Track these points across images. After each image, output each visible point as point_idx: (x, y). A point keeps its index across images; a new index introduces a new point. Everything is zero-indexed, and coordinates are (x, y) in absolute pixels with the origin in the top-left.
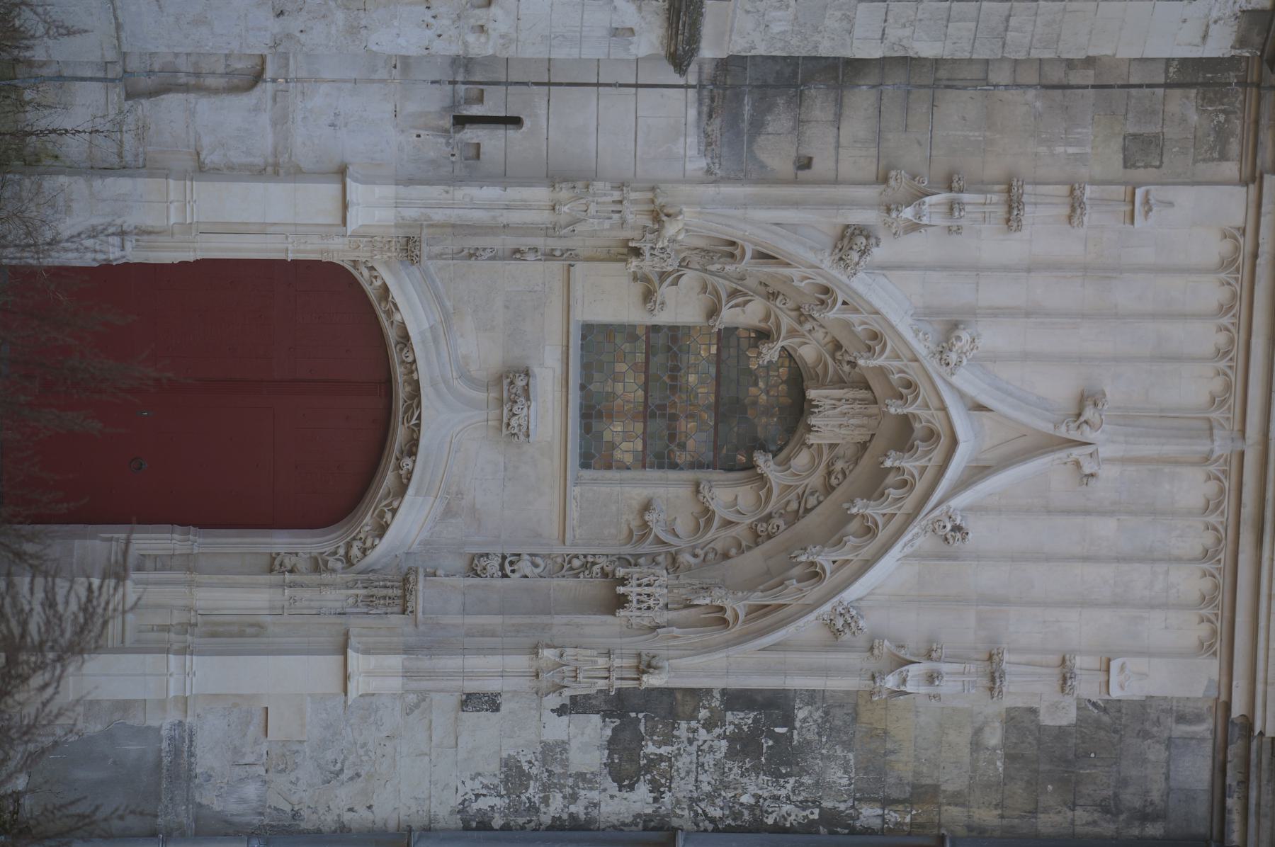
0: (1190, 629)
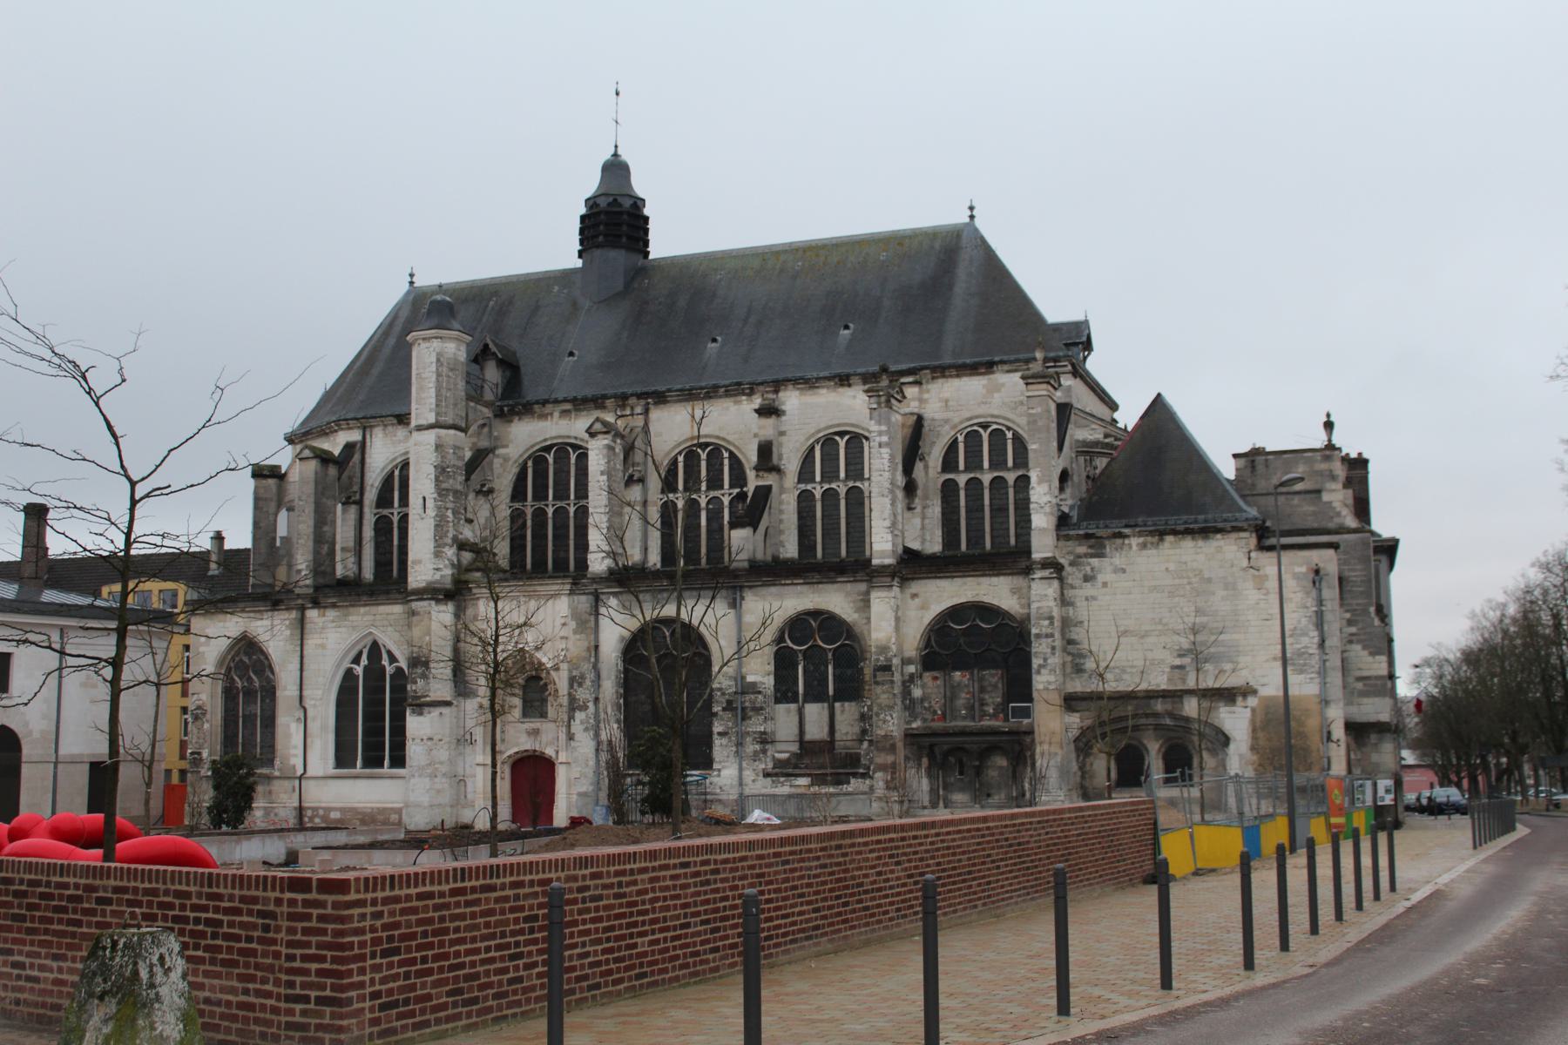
0: (558, 602)
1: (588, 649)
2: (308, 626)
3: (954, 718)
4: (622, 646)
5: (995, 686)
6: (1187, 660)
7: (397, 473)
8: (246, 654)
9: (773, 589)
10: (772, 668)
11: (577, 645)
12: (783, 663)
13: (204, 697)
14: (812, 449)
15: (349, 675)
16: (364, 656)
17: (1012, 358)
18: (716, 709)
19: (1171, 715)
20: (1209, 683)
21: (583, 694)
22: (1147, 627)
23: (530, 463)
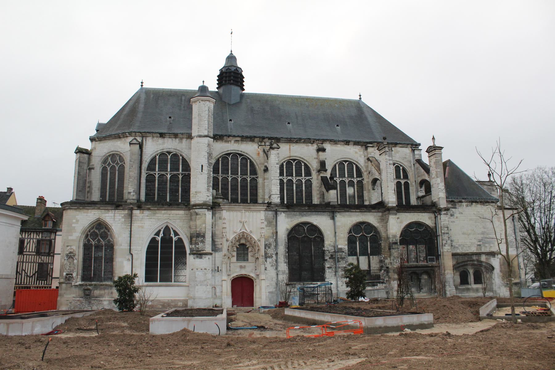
0: (259, 214)
1: (273, 233)
2: (134, 218)
3: (411, 262)
4: (287, 232)
5: (423, 251)
6: (481, 243)
7: (157, 157)
8: (96, 229)
9: (347, 213)
10: (346, 243)
11: (268, 231)
12: (351, 241)
13: (74, 247)
14: (335, 165)
15: (153, 241)
16: (162, 232)
17: (403, 142)
18: (327, 258)
19: (478, 261)
20: (487, 250)
21: (271, 251)
22: (470, 232)
23: (220, 159)
